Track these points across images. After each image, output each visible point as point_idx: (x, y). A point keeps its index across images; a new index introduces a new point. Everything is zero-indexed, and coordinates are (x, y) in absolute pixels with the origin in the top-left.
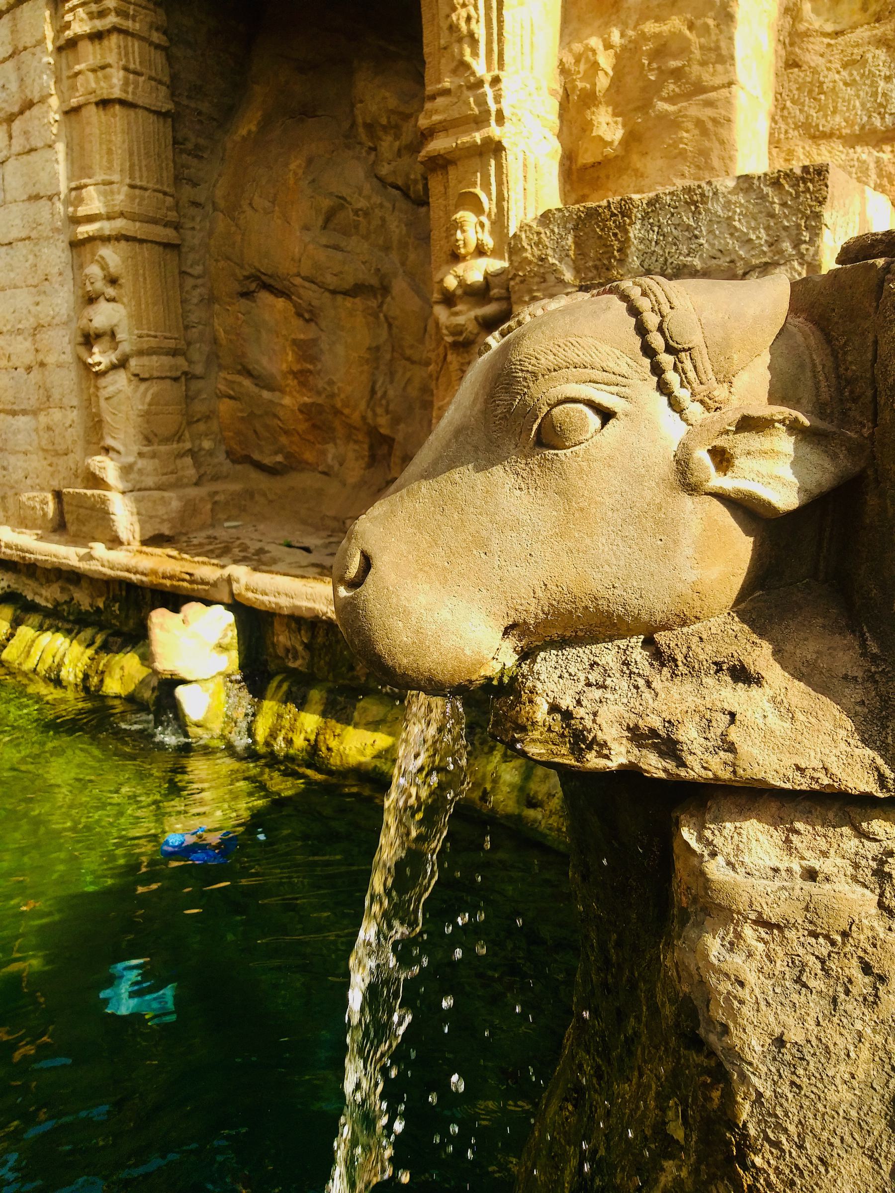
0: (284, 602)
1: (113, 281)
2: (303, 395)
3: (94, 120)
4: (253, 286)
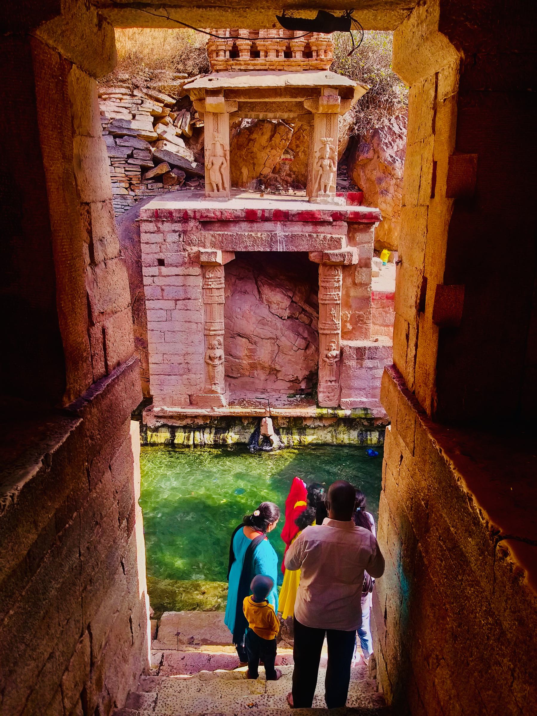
0: (287, 414)
1: (220, 344)
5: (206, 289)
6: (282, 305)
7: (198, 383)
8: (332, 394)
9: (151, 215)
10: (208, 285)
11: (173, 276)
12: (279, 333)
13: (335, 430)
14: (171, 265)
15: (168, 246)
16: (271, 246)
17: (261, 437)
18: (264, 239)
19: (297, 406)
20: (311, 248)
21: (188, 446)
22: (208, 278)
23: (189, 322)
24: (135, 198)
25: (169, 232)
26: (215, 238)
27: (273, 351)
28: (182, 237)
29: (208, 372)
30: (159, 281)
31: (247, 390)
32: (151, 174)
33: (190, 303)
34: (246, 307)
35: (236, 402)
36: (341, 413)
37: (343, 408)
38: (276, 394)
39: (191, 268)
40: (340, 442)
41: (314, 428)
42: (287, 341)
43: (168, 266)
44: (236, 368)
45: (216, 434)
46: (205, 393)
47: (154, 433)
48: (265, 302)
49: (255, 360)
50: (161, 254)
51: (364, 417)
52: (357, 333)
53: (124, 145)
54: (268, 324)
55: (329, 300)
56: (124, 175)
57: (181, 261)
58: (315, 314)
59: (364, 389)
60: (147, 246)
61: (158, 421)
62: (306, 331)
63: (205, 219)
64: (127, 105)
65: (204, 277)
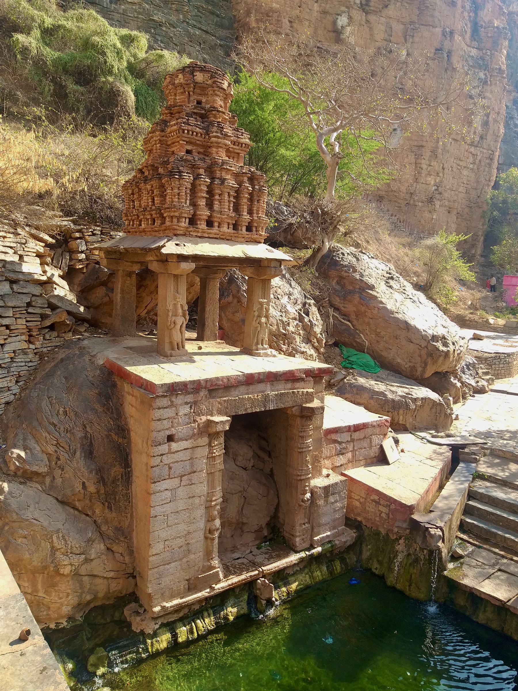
5: (211, 458)
8: (306, 536)
9: (167, 389)
10: (212, 453)
14: (181, 440)
15: (180, 419)
23: (193, 497)
24: (35, 351)
25: (181, 405)
26: (221, 405)
29: (207, 547)
30: (166, 460)
32: (48, 323)
33: (194, 476)
36: (314, 551)
39: (200, 439)
41: (293, 575)
43: (178, 441)
46: (204, 572)
47: (154, 640)
50: (173, 429)
53: (21, 291)
56: (25, 327)
57: (191, 433)
60: (159, 423)
61: (156, 624)
63: (214, 388)
64: (12, 245)
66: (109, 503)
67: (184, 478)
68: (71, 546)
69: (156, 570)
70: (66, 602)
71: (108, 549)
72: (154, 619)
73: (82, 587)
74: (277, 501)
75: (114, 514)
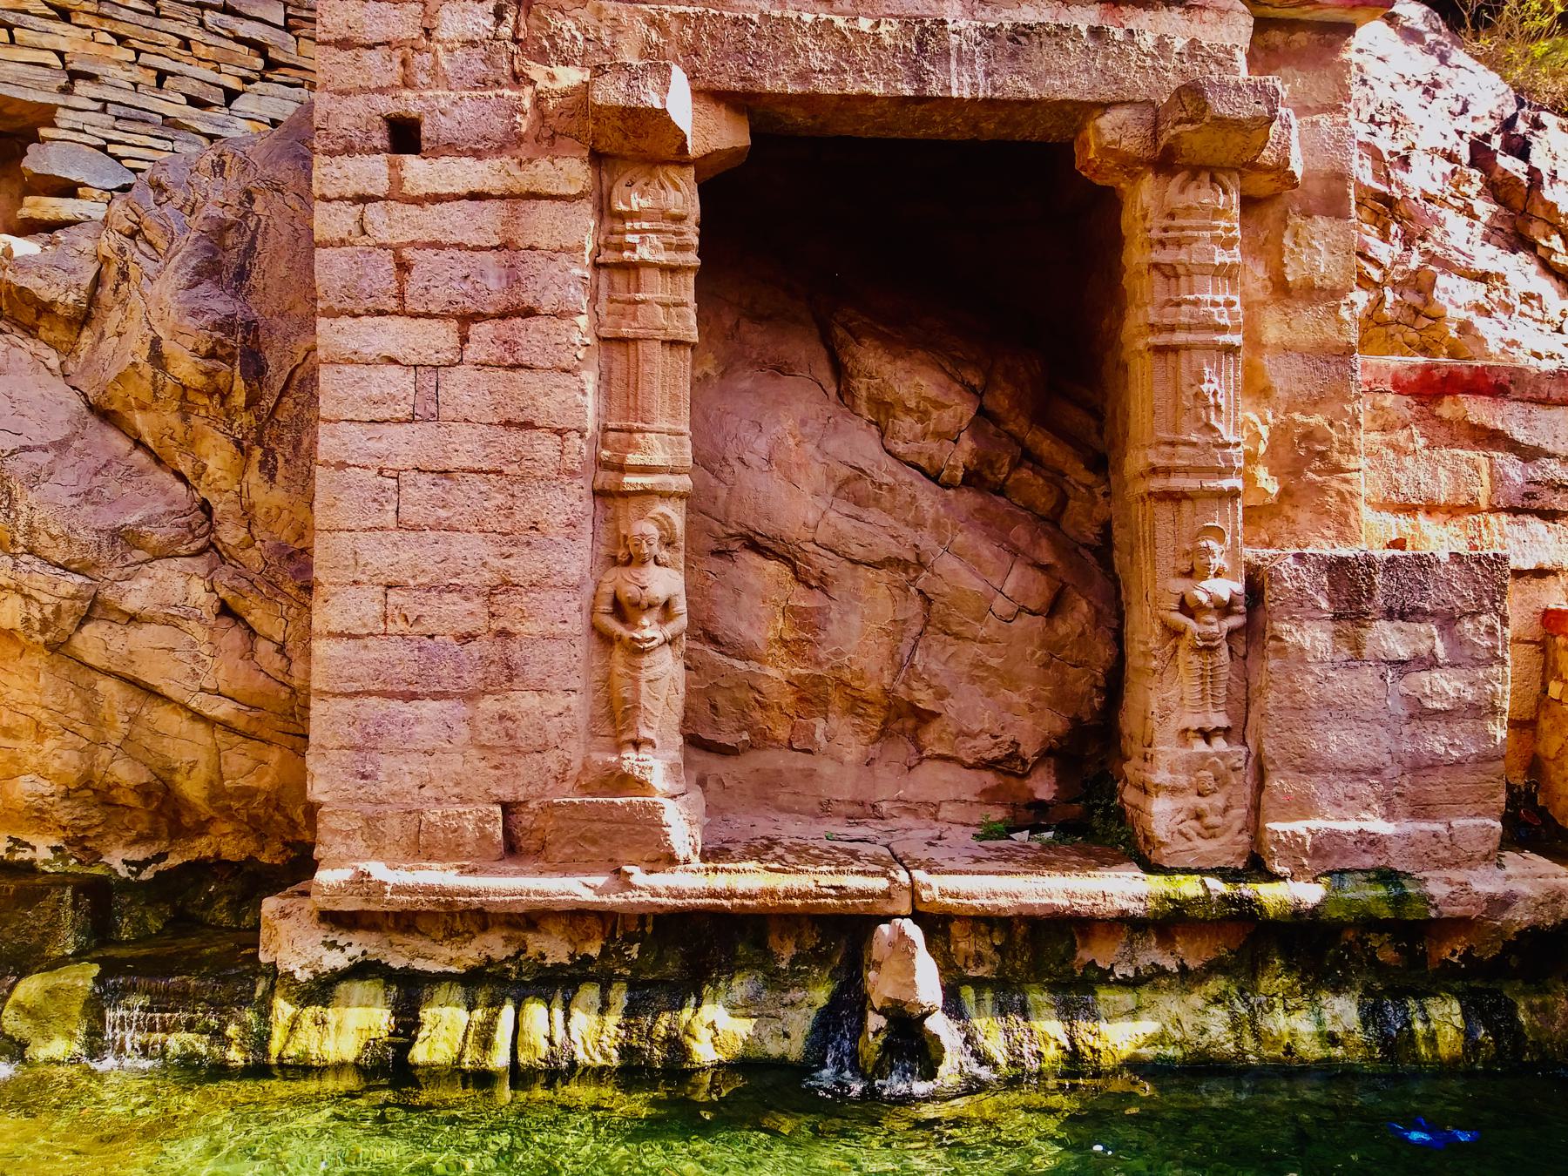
0: (1003, 902)
1: (669, 544)
2: (794, 666)
3: (659, 359)
4: (736, 546)
5: (616, 268)
6: (940, 419)
7: (553, 737)
8: (1219, 800)
10: (620, 248)
11: (457, 197)
12: (927, 541)
13: (1242, 991)
14: (451, 148)
15: (443, 58)
16: (918, 77)
17: (875, 1021)
18: (888, 41)
19: (1040, 862)
20: (1103, 88)
21: (483, 1079)
22: (622, 217)
23: (528, 425)
27: (900, 624)
28: (511, 20)
29: (607, 681)
30: (389, 224)
31: (782, 810)
33: (530, 334)
34: (784, 425)
35: (737, 850)
37: (1278, 869)
38: (920, 824)
39: (544, 164)
40: (1279, 1052)
42: (965, 574)
43: (436, 153)
44: (734, 701)
45: (631, 1011)
46: (586, 789)
47: (311, 1011)
48: (864, 411)
49: (819, 664)
50: (406, 93)
51: (1386, 913)
52: (1303, 517)
54: (877, 500)
55: (1189, 328)
57: (498, 126)
58: (1078, 474)
59: (1376, 771)
60: (344, 56)
62: (1044, 542)
65: (604, 210)
66: (269, 452)
67: (480, 330)
68: (30, 524)
69: (347, 705)
70: (33, 760)
71: (225, 610)
72: (337, 920)
73: (92, 715)
74: (1105, 653)
75: (278, 496)
